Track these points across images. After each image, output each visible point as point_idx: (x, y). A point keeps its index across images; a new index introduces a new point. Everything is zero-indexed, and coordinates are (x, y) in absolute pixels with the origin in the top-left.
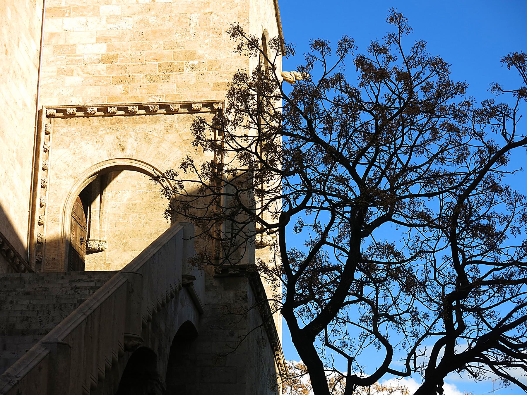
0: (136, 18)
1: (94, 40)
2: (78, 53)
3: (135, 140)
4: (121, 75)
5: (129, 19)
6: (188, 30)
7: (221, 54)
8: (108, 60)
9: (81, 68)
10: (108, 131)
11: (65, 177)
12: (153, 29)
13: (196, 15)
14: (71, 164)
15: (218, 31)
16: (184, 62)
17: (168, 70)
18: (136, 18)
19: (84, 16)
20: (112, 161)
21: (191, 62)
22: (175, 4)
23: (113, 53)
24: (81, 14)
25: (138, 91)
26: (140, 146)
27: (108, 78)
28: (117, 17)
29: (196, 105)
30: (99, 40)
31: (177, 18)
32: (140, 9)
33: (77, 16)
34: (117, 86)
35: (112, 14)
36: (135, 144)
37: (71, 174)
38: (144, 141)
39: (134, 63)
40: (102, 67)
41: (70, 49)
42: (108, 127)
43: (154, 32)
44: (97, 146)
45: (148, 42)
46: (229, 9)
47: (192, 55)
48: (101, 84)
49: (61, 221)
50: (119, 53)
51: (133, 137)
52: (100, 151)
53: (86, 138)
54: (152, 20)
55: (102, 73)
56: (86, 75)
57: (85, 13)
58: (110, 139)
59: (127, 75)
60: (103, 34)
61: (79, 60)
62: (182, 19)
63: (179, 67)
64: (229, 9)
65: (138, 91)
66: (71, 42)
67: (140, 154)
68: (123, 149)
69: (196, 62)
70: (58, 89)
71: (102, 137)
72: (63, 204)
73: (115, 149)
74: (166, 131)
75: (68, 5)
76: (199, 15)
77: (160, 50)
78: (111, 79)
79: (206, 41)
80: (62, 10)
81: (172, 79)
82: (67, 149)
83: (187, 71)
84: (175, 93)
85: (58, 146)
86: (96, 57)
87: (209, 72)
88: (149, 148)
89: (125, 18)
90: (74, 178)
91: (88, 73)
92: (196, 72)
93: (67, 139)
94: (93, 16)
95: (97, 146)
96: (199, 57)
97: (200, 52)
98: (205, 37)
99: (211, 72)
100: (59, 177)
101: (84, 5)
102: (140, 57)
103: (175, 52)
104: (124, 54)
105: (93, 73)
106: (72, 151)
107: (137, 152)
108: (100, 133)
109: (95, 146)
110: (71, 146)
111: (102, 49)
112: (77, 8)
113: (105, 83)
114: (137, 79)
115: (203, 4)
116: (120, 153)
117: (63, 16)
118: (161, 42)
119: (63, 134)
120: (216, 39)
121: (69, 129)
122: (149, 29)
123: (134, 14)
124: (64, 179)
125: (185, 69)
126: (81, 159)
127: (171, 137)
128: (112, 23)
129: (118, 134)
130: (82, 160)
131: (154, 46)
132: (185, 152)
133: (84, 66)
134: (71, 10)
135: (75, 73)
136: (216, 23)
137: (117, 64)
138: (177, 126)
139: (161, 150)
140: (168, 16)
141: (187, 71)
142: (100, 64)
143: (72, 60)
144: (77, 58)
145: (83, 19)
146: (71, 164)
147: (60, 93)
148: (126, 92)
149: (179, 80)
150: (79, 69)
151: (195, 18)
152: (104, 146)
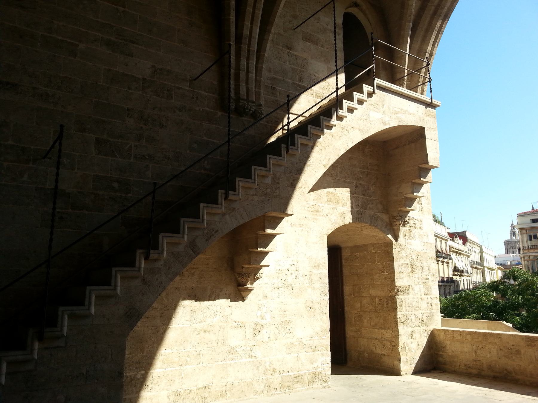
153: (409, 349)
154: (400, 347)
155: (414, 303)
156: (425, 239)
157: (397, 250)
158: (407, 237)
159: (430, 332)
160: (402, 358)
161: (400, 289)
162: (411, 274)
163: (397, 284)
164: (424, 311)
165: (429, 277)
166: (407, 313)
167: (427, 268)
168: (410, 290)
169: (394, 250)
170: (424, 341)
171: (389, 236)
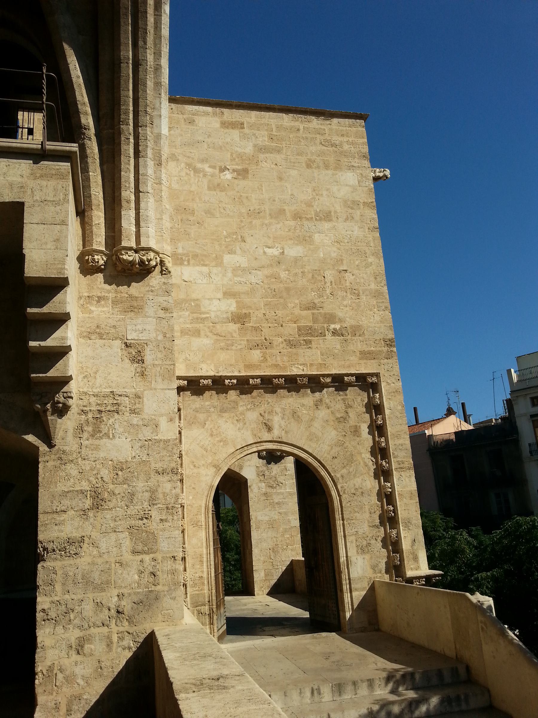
0: (267, 272)
1: (220, 295)
2: (203, 309)
3: (283, 418)
4: (256, 338)
5: (259, 272)
6: (324, 289)
7: (363, 318)
8: (240, 318)
9: (209, 328)
10: (249, 407)
11: (203, 465)
12: (286, 285)
13: (330, 272)
14: (209, 449)
15: (356, 292)
16: (325, 325)
17: (307, 335)
18: (267, 272)
19: (206, 265)
20: (258, 445)
21: (332, 326)
22: (306, 258)
23: (244, 311)
24: (202, 263)
25: (279, 358)
26: (289, 425)
27: (242, 342)
28: (244, 270)
29: (350, 378)
30: (228, 294)
31: (310, 275)
32: (268, 262)
33: (197, 265)
34: (253, 351)
35: (238, 265)
36: (283, 423)
38: (293, 419)
39: (270, 325)
40: (233, 327)
41: (193, 304)
42: (248, 401)
43: (288, 289)
44: (238, 425)
45: (282, 301)
46: (364, 268)
47: (331, 318)
48: (234, 348)
49: (203, 523)
50: (251, 311)
51: (280, 415)
52: (242, 432)
53: (224, 415)
54: (283, 275)
55: (235, 335)
56: (215, 337)
57: (207, 263)
58: (252, 416)
59: (263, 338)
60: (230, 289)
61: (205, 318)
62: (316, 276)
63: (320, 331)
64: (364, 268)
65: (279, 358)
66: (194, 296)
68: (269, 429)
69: (338, 327)
70: (184, 353)
71: (242, 414)
72: (204, 502)
73: (260, 430)
74: (315, 407)
75: (185, 252)
76: (333, 272)
77: (297, 311)
78: (245, 342)
79: (345, 303)
80: (180, 257)
81: (314, 345)
82: (203, 430)
83: (329, 336)
84: (320, 361)
85: (191, 425)
86: (225, 316)
87: (353, 338)
88: (300, 428)
89: (254, 271)
90: (215, 466)
91: (217, 334)
92: (339, 338)
93: (201, 417)
94: (216, 266)
96: (341, 321)
97: (340, 314)
98: (343, 298)
99: (355, 338)
100: (197, 466)
101: (205, 253)
102: (276, 318)
103: (313, 314)
104: (257, 312)
105: (224, 335)
106: (209, 431)
107: (286, 432)
108: (241, 409)
109: (236, 425)
110: (207, 426)
111: (231, 306)
112: (197, 256)
113: (239, 347)
114: (275, 343)
115: (336, 260)
116: (266, 434)
117: (182, 264)
118: (297, 301)
119: (196, 411)
120: (355, 301)
121: (202, 403)
122: (282, 285)
123: (263, 267)
124: (203, 468)
125: (327, 334)
126: (221, 442)
127: (323, 413)
128: (239, 276)
129: (261, 410)
130: (222, 443)
131: (289, 305)
132: (340, 432)
133: (212, 326)
134: (190, 257)
135: (202, 333)
136: (353, 283)
137: (250, 325)
138: (327, 401)
140: (300, 272)
141: (329, 336)
142: (230, 324)
143: (197, 319)
144: (204, 316)
145: (205, 269)
146: (209, 449)
147: (186, 358)
148: (265, 360)
149: (322, 346)
150: (207, 330)
151: (330, 275)
152: (246, 426)
153: (66, 678)
154: (40, 675)
155: (96, 575)
156: (147, 433)
157: (51, 464)
158: (85, 435)
159: (144, 636)
160: (41, 699)
161: (50, 546)
162: (91, 514)
163: (41, 537)
164: (126, 591)
165: (154, 513)
166: (67, 596)
167: (147, 495)
168: (85, 546)
169: (41, 466)
170: (120, 657)
171: (30, 438)
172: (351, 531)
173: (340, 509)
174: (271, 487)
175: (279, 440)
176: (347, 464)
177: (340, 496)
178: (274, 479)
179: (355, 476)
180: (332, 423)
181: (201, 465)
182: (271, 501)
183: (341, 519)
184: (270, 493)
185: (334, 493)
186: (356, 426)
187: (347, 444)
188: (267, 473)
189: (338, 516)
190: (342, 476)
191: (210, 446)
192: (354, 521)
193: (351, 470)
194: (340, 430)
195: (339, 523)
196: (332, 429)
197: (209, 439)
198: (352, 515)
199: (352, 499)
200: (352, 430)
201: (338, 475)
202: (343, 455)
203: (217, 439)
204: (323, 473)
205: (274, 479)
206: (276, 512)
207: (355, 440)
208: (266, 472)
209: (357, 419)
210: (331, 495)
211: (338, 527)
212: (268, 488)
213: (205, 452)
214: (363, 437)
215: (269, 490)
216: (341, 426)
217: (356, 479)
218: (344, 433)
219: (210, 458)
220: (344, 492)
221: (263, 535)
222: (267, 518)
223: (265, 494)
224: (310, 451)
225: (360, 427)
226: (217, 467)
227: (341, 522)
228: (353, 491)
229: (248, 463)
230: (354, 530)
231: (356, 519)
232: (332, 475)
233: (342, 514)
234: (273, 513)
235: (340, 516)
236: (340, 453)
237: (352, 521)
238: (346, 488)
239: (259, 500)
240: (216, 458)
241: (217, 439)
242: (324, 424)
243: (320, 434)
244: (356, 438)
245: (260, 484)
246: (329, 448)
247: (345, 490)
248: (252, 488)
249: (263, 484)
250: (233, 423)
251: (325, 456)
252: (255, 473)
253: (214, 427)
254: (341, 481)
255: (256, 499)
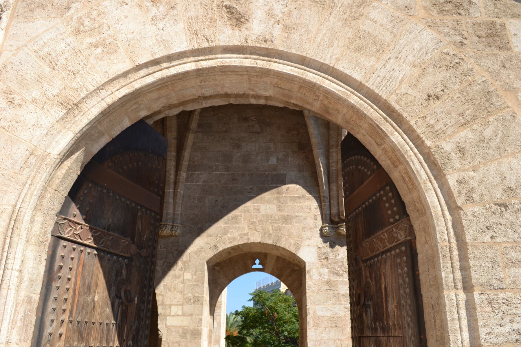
11: (35, 101)
14: (62, 61)
26: (295, 13)
37: (55, 92)
52: (161, 25)
67: (295, 37)
68: (238, 19)
73: (212, 20)
82: (59, 20)
85: (32, 10)
88: (327, 20)
95: (154, 11)
100: (17, 101)
107: (287, 28)
110: (71, 11)
116: (229, 31)
124: (32, 107)
126: (97, 46)
130: (99, 50)
132: (448, 34)
139: (366, 26)
146: (62, 61)
152: (175, 12)
172: (499, 330)
173: (456, 253)
174: (337, 274)
175: (265, 45)
176: (475, 117)
177: (454, 208)
178: (340, 264)
179: (501, 151)
180: (422, 13)
181: (29, 99)
182: (336, 292)
183: (460, 285)
184: (334, 281)
185: (433, 199)
186: (492, 25)
187: (470, 63)
188: (331, 256)
189: (449, 274)
190: (461, 150)
191: (67, 55)
192: (508, 294)
193: (488, 132)
194: (446, 30)
195: (453, 298)
196: (420, 26)
197: (68, 41)
198: (501, 275)
199: (495, 219)
200: (483, 33)
201: (448, 147)
202: (461, 92)
203: (90, 40)
204: (397, 137)
205: (340, 264)
206: (342, 306)
207: (495, 55)
208: (331, 255)
209: (492, 7)
210: (424, 210)
211: (451, 314)
212: (332, 275)
213: (48, 70)
214: (516, 50)
215: (333, 278)
216: (450, 20)
217: (506, 160)
218: (458, 38)
219: (60, 83)
220: (470, 199)
221: (323, 335)
222: (329, 314)
223: (328, 282)
224: (357, 76)
225: (503, 25)
226: (72, 108)
227: (462, 296)
228: (499, 195)
229: (307, 242)
230: (508, 328)
231: (514, 286)
232: (428, 143)
233: (465, 269)
234: (338, 307)
235: (458, 274)
236: (448, 84)
237: (501, 295)
238: (474, 183)
239: (319, 290)
240: (75, 85)
241: (90, 40)
242: (398, 14)
243: (388, 37)
244: (496, 51)
245: (321, 270)
246: (416, 72)
247: (472, 190)
248: (311, 273)
249: (326, 270)
250: (140, 7)
251: (403, 91)
252: (316, 255)
253: (90, 14)
254: (456, 162)
255: (316, 289)
